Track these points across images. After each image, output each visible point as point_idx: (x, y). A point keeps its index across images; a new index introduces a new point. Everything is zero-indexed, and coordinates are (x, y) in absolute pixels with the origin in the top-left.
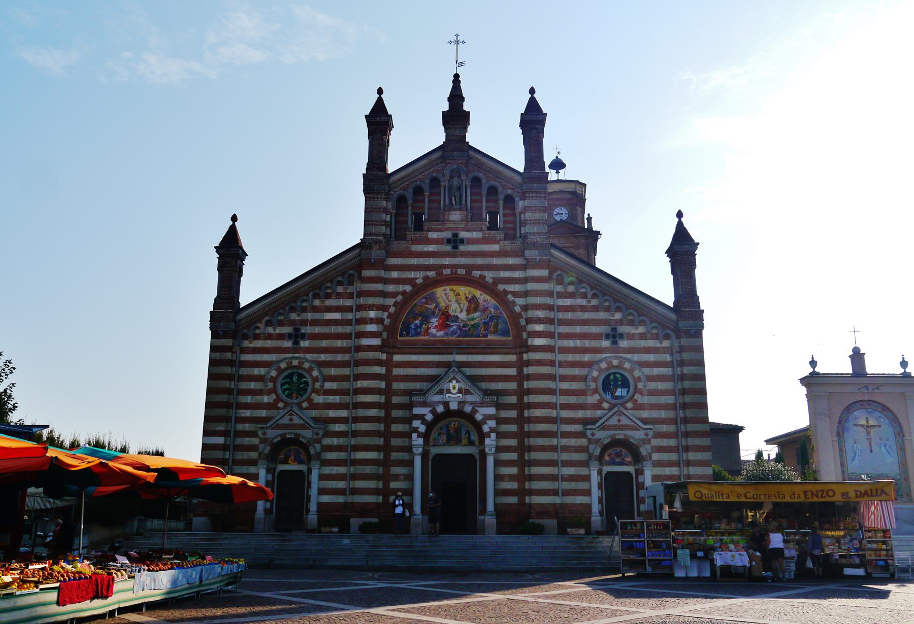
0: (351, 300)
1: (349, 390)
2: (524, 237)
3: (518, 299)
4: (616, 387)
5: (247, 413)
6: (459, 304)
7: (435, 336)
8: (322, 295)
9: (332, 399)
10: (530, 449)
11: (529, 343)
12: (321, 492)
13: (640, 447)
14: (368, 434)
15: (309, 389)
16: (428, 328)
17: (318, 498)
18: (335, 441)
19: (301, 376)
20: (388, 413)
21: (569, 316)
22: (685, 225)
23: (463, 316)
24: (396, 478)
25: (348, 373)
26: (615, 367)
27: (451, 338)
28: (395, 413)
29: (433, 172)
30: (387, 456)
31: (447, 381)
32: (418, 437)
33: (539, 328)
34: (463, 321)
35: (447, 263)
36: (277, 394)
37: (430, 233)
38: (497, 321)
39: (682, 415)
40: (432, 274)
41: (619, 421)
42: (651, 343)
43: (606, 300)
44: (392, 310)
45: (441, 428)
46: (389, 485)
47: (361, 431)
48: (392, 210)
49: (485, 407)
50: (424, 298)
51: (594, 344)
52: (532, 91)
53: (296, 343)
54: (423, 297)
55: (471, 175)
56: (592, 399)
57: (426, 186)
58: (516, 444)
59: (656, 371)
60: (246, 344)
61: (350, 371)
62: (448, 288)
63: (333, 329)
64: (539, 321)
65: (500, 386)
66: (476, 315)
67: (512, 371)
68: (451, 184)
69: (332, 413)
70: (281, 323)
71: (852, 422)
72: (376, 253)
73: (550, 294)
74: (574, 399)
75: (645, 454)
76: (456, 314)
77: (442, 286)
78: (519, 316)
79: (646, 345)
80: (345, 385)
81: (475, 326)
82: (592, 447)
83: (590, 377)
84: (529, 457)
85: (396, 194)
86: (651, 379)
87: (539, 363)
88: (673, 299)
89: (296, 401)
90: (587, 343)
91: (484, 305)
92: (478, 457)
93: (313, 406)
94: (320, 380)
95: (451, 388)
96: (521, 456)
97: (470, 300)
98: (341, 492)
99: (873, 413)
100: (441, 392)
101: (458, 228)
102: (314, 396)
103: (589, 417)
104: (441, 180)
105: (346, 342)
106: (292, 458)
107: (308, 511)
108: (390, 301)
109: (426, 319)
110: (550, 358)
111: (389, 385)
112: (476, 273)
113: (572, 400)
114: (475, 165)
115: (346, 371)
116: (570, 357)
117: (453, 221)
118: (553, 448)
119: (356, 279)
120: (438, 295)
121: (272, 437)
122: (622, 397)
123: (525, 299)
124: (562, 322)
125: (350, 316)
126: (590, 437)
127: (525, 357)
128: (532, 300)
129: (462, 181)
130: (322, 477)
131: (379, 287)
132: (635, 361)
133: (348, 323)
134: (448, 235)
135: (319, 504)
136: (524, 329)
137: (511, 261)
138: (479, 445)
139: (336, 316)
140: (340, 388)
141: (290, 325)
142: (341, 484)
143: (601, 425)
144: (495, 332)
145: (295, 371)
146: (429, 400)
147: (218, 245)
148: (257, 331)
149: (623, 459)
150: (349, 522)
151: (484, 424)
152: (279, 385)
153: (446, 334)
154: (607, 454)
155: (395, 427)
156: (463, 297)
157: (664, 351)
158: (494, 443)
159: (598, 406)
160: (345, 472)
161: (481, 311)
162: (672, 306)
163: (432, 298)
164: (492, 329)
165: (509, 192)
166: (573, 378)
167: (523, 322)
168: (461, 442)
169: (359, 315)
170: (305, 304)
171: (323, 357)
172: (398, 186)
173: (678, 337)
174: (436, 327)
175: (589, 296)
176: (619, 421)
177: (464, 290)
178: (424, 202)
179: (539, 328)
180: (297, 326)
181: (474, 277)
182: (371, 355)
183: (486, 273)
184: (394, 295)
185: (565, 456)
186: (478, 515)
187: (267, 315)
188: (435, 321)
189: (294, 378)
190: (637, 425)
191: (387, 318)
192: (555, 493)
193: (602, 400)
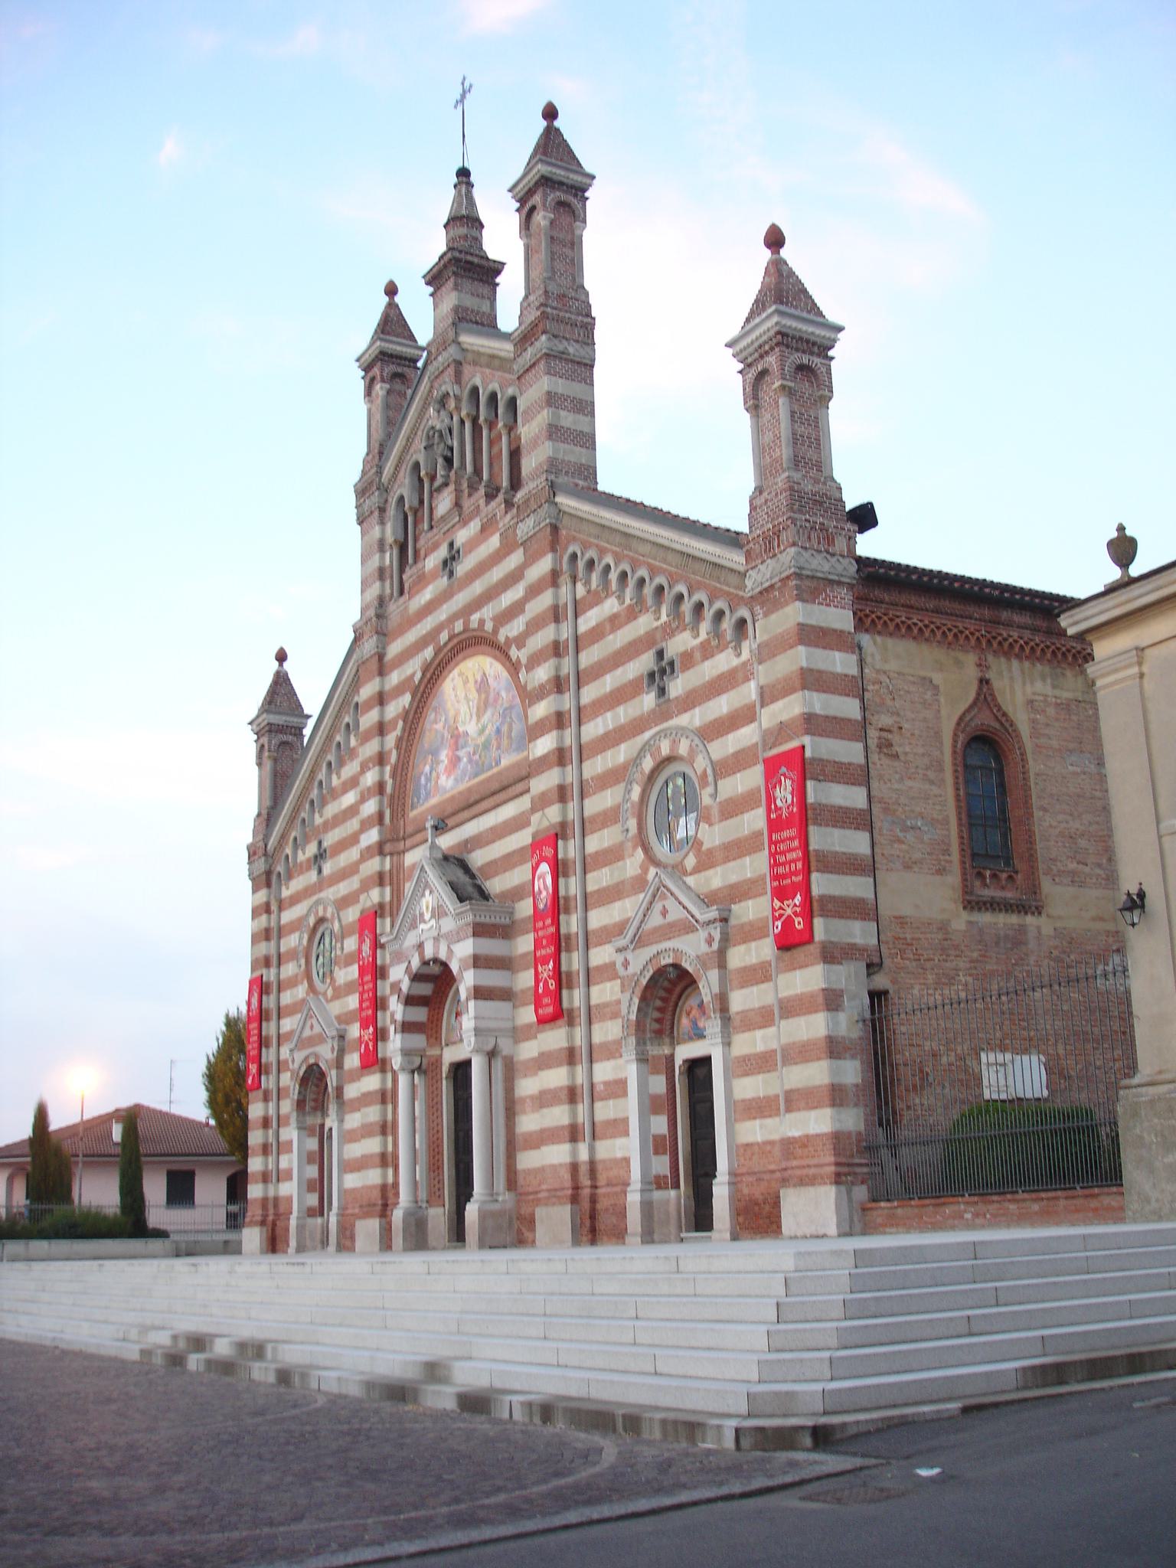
52: (550, 113)
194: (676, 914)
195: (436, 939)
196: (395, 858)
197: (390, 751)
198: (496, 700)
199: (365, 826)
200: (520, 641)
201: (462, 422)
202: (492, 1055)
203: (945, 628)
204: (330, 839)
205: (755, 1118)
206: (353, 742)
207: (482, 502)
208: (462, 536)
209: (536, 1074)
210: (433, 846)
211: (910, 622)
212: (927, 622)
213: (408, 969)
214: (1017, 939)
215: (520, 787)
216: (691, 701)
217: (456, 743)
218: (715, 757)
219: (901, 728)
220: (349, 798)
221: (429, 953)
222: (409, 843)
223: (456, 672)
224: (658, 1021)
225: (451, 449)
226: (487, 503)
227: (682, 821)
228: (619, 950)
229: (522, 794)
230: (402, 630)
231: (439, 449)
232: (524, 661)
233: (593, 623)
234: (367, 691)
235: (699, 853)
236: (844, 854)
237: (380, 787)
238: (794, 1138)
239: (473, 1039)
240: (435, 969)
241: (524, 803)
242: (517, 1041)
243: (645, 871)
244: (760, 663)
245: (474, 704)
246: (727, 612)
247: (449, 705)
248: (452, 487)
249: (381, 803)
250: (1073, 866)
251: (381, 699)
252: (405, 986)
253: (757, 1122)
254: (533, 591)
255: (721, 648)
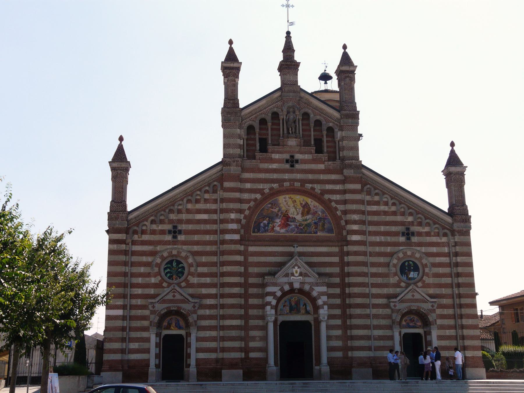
0: (216, 205)
1: (217, 273)
2: (343, 159)
3: (339, 205)
4: (410, 271)
5: (139, 291)
6: (296, 208)
7: (279, 232)
8: (194, 201)
9: (203, 280)
10: (351, 317)
11: (349, 239)
12: (198, 350)
13: (429, 315)
14: (232, 306)
15: (186, 272)
16: (274, 227)
17: (196, 356)
18: (208, 312)
19: (178, 263)
20: (246, 291)
21: (376, 218)
22: (457, 152)
23: (299, 217)
24: (253, 339)
25: (215, 261)
26: (409, 256)
27: (291, 234)
28: (252, 291)
29: (274, 107)
30: (246, 322)
31: (291, 267)
32: (272, 308)
33: (355, 227)
34: (299, 221)
35: (287, 178)
36: (161, 277)
37: (273, 155)
38: (324, 221)
39: (457, 292)
40: (275, 186)
42: (435, 239)
43: (402, 207)
44: (247, 212)
45: (285, 302)
46: (249, 345)
47: (228, 305)
48: (245, 136)
49: (319, 286)
50: (270, 203)
51: (394, 239)
52: (345, 47)
53: (175, 237)
54: (269, 203)
55: (303, 111)
56: (393, 280)
57: (269, 118)
58: (340, 313)
59: (438, 260)
60: (136, 237)
61: (217, 259)
62: (287, 196)
63: (202, 227)
64: (355, 222)
65: (328, 270)
66: (309, 217)
67: (336, 259)
68: (288, 117)
69: (204, 291)
70: (162, 222)
72: (234, 169)
73: (362, 202)
74: (380, 280)
75: (432, 320)
76: (294, 216)
77: (283, 195)
78: (340, 218)
79: (431, 241)
80: (214, 269)
81: (308, 225)
82: (394, 316)
83: (391, 264)
84: (351, 322)
85: (247, 124)
86: (434, 265)
87: (356, 253)
88: (448, 207)
89: (175, 281)
90: (389, 239)
91: (314, 210)
92: (312, 323)
93: (190, 285)
94: (194, 265)
95: (294, 272)
96: (344, 322)
97: (304, 205)
98: (214, 350)
100: (287, 275)
101: (294, 151)
102: (190, 278)
103: (392, 293)
104: (280, 114)
105: (213, 237)
106: (174, 324)
107: (189, 366)
108: (245, 206)
109: (271, 219)
110: (363, 250)
111: (246, 269)
112: (309, 186)
113: (379, 280)
114: (305, 103)
115: (214, 259)
116: (377, 249)
117: (291, 146)
118: (367, 316)
119: (219, 189)
120: (280, 202)
121: (160, 310)
122: (414, 278)
123: (344, 205)
124: (371, 223)
125: (215, 217)
126: (393, 308)
127: (345, 249)
128: (350, 207)
129: (296, 116)
130: (198, 339)
131: (237, 195)
132: (423, 252)
133: (214, 222)
134: (287, 156)
135: (197, 360)
136: (344, 228)
137: (334, 177)
138: (314, 314)
139: (205, 217)
140: (209, 271)
141: (169, 223)
142: (213, 345)
143: (401, 299)
144: (323, 230)
145: (174, 258)
146: (278, 281)
147: (111, 161)
148: (144, 228)
149: (415, 323)
150: (221, 373)
151: (319, 299)
152: (162, 270)
153: (287, 231)
154: (404, 320)
155: (251, 301)
156: (298, 203)
157: (442, 245)
158: (326, 312)
159: (397, 285)
160: (216, 335)
161: (312, 214)
162: (447, 211)
163: (275, 204)
164: (320, 228)
165: (331, 125)
166: (379, 265)
167: (343, 223)
168: (300, 312)
169: (223, 216)
170: (180, 207)
171: (196, 248)
172: (248, 118)
173: (453, 235)
174: (279, 226)
175: (390, 204)
176: (413, 296)
177: (299, 198)
178: (267, 129)
179: (355, 227)
180: (175, 224)
181: (306, 189)
182: (233, 247)
183: (315, 186)
184: (248, 201)
185: (375, 322)
186: (314, 365)
187: (152, 216)
188: (278, 221)
189: (174, 264)
190: (426, 299)
191: (244, 219)
192: (369, 349)
193: (400, 281)
253: (447, 352)
255: (438, 236)
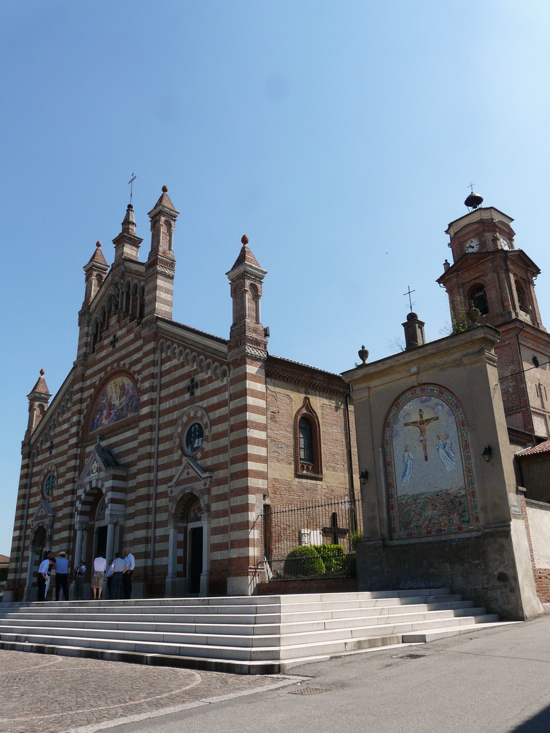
40: (102, 374)
41: (188, 473)
71: (402, 421)
99: (428, 401)
194: (192, 474)
195: (97, 480)
196: (82, 449)
197: (84, 410)
198: (127, 393)
199: (71, 436)
200: (139, 372)
201: (123, 293)
202: (115, 524)
203: (295, 379)
204: (56, 441)
205: (218, 551)
206: (69, 405)
207: (128, 321)
208: (119, 333)
209: (133, 532)
210: (99, 445)
211: (283, 375)
212: (289, 376)
213: (85, 492)
214: (314, 489)
215: (134, 425)
216: (203, 397)
217: (110, 408)
218: (211, 418)
219: (278, 412)
220: (65, 426)
221: (94, 485)
222: (88, 443)
223: (112, 382)
224: (182, 513)
225: (118, 302)
226: (130, 322)
227: (197, 440)
228: (169, 487)
229: (135, 428)
230: (92, 365)
231: (114, 302)
232: (140, 379)
233: (168, 368)
234: (76, 387)
235: (202, 452)
236: (257, 455)
237: (78, 423)
238: (234, 558)
239: (109, 518)
240: (95, 491)
241: (136, 431)
242: (126, 520)
243: (181, 458)
244: (231, 385)
245: (118, 394)
246: (220, 367)
247: (108, 394)
248: (117, 315)
249: (78, 428)
250: (333, 465)
251: (82, 390)
252: (83, 497)
253: (219, 552)
254: (146, 354)
255: (217, 379)
